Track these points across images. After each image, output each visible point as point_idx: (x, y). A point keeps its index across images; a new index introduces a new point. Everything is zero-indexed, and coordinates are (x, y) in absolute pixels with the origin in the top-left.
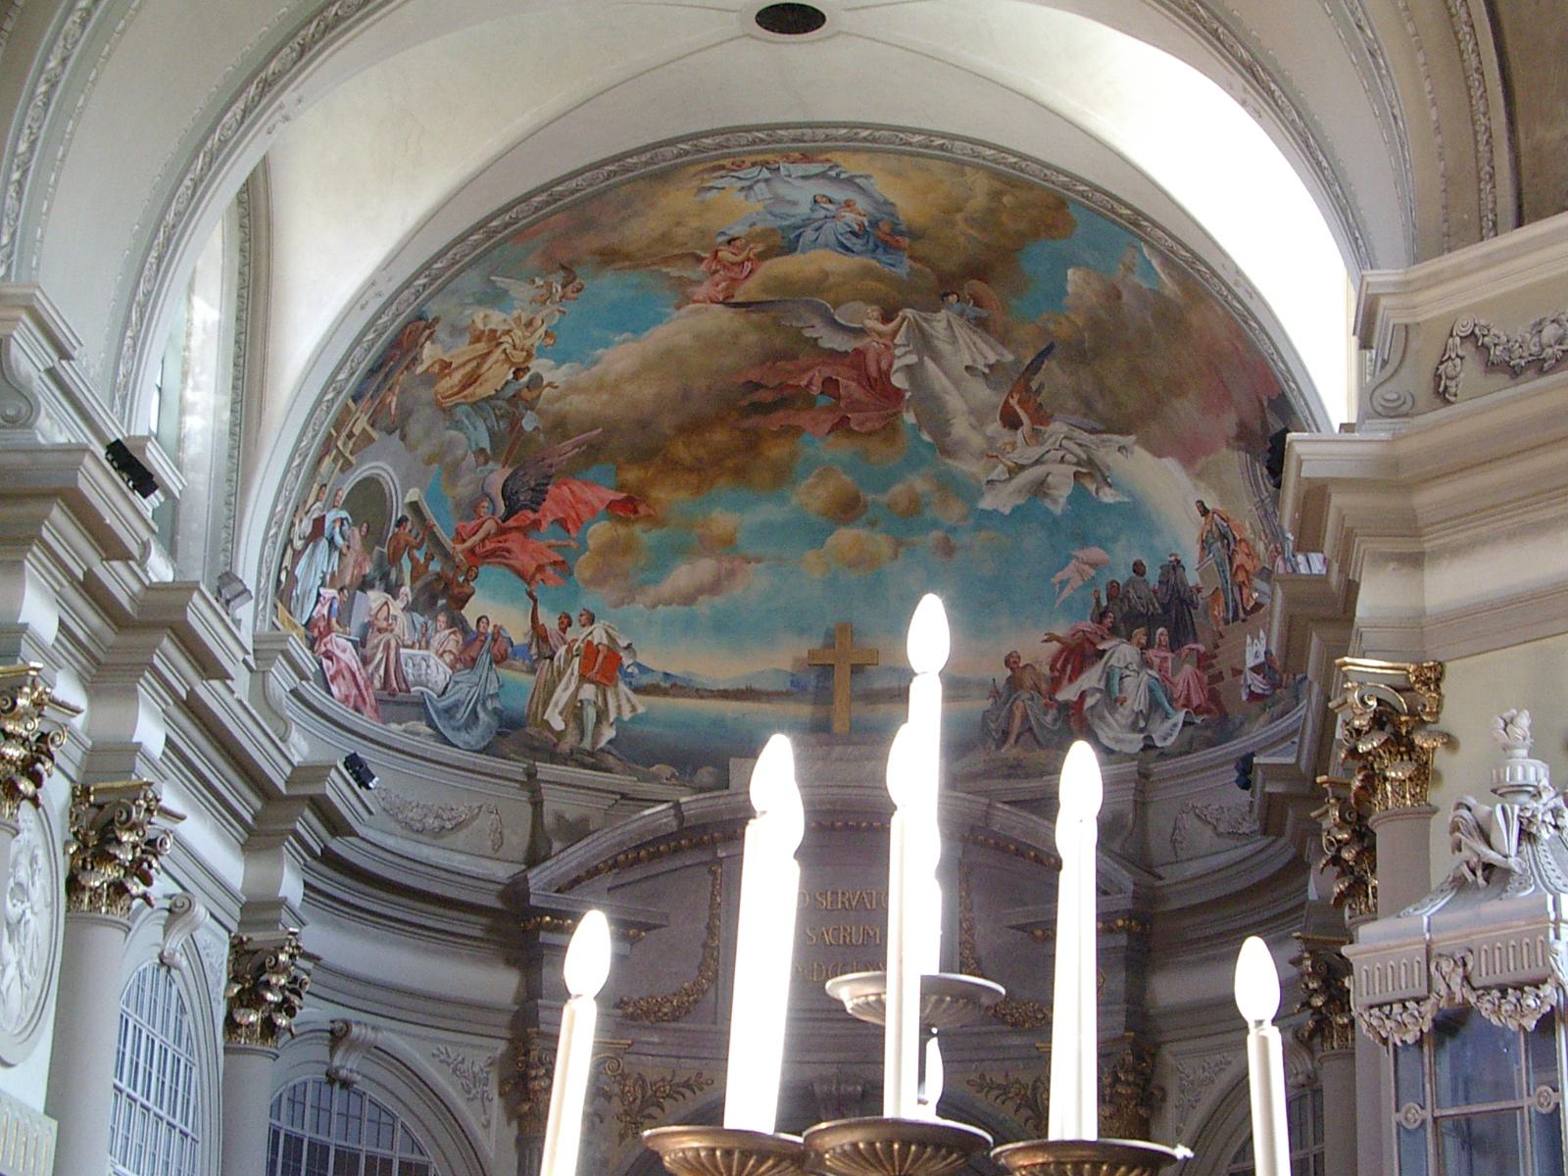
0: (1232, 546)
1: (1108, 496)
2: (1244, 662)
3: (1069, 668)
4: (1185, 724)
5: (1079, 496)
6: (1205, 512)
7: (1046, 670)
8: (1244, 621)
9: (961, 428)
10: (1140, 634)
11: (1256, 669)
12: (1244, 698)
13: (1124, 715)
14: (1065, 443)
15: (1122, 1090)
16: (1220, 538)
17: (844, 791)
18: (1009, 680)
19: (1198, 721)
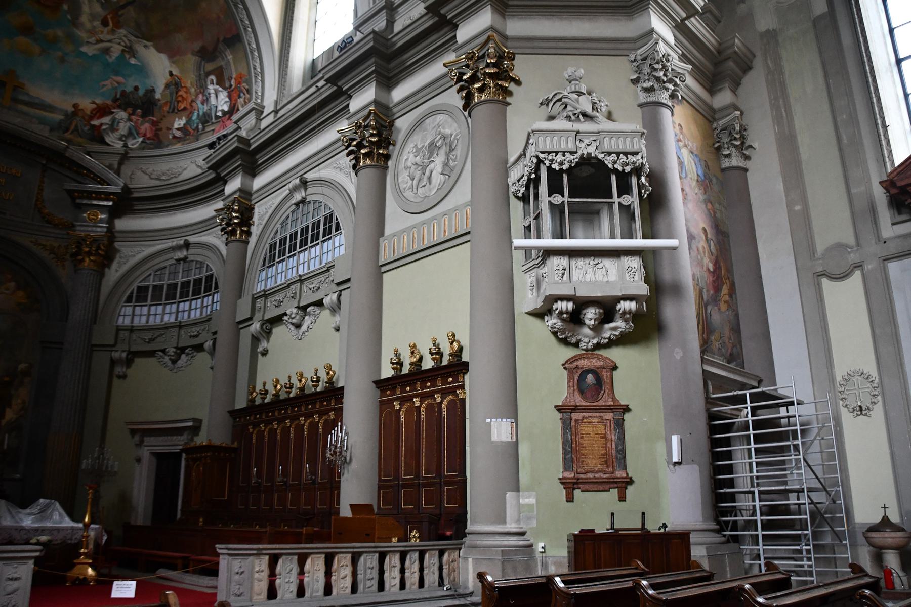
0: (179, 88)
1: (133, 61)
2: (173, 126)
3: (98, 115)
4: (142, 142)
5: (121, 57)
6: (171, 74)
7: (88, 113)
8: (176, 113)
9: (84, 19)
10: (130, 110)
11: (178, 129)
12: (171, 137)
13: (117, 134)
14: (124, 39)
15: (100, 252)
16: (175, 85)
17: (7, 124)
18: (73, 112)
19: (148, 142)
